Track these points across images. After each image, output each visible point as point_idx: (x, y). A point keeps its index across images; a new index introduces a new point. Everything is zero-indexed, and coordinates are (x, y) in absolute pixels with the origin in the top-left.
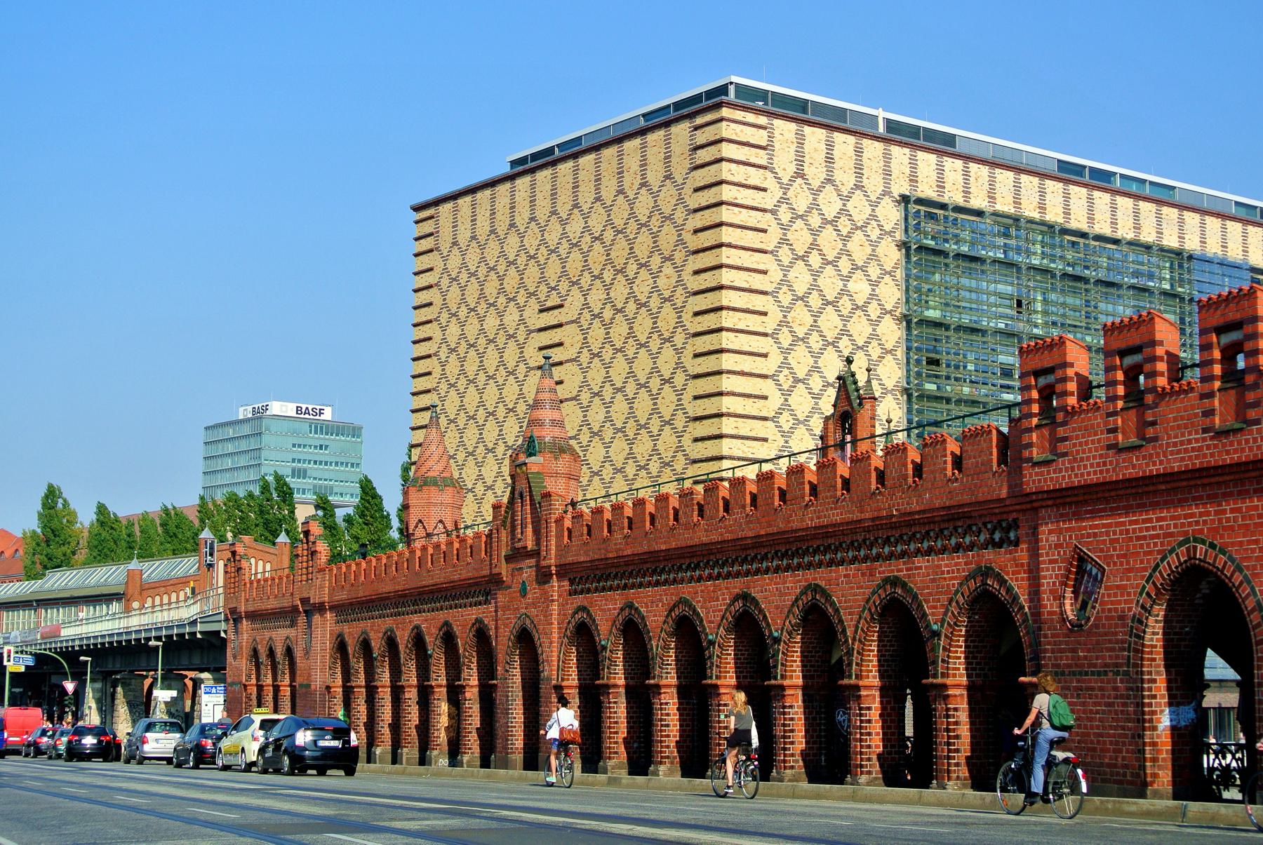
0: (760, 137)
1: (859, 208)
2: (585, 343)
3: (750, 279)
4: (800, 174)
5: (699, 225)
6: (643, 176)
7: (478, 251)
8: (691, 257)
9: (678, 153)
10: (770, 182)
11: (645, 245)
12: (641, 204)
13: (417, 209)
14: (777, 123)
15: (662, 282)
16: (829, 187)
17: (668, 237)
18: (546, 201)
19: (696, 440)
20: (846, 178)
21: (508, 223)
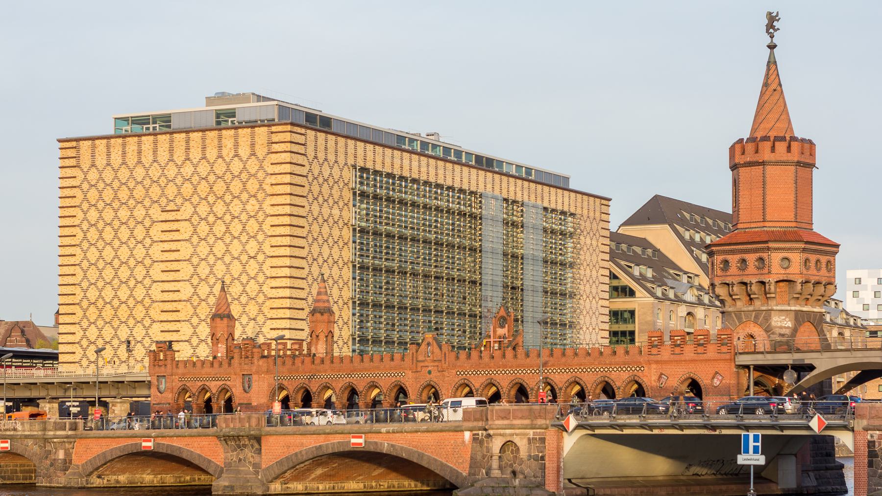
0: (301, 139)
1: (336, 172)
2: (195, 231)
3: (298, 210)
4: (316, 157)
5: (274, 182)
6: (236, 151)
7: (112, 172)
8: (269, 198)
9: (260, 142)
10: (305, 163)
11: (238, 187)
12: (235, 166)
13: (60, 141)
14: (309, 131)
15: (249, 207)
16: (326, 163)
17: (253, 185)
18: (166, 153)
19: (272, 288)
20: (331, 157)
21: (136, 160)
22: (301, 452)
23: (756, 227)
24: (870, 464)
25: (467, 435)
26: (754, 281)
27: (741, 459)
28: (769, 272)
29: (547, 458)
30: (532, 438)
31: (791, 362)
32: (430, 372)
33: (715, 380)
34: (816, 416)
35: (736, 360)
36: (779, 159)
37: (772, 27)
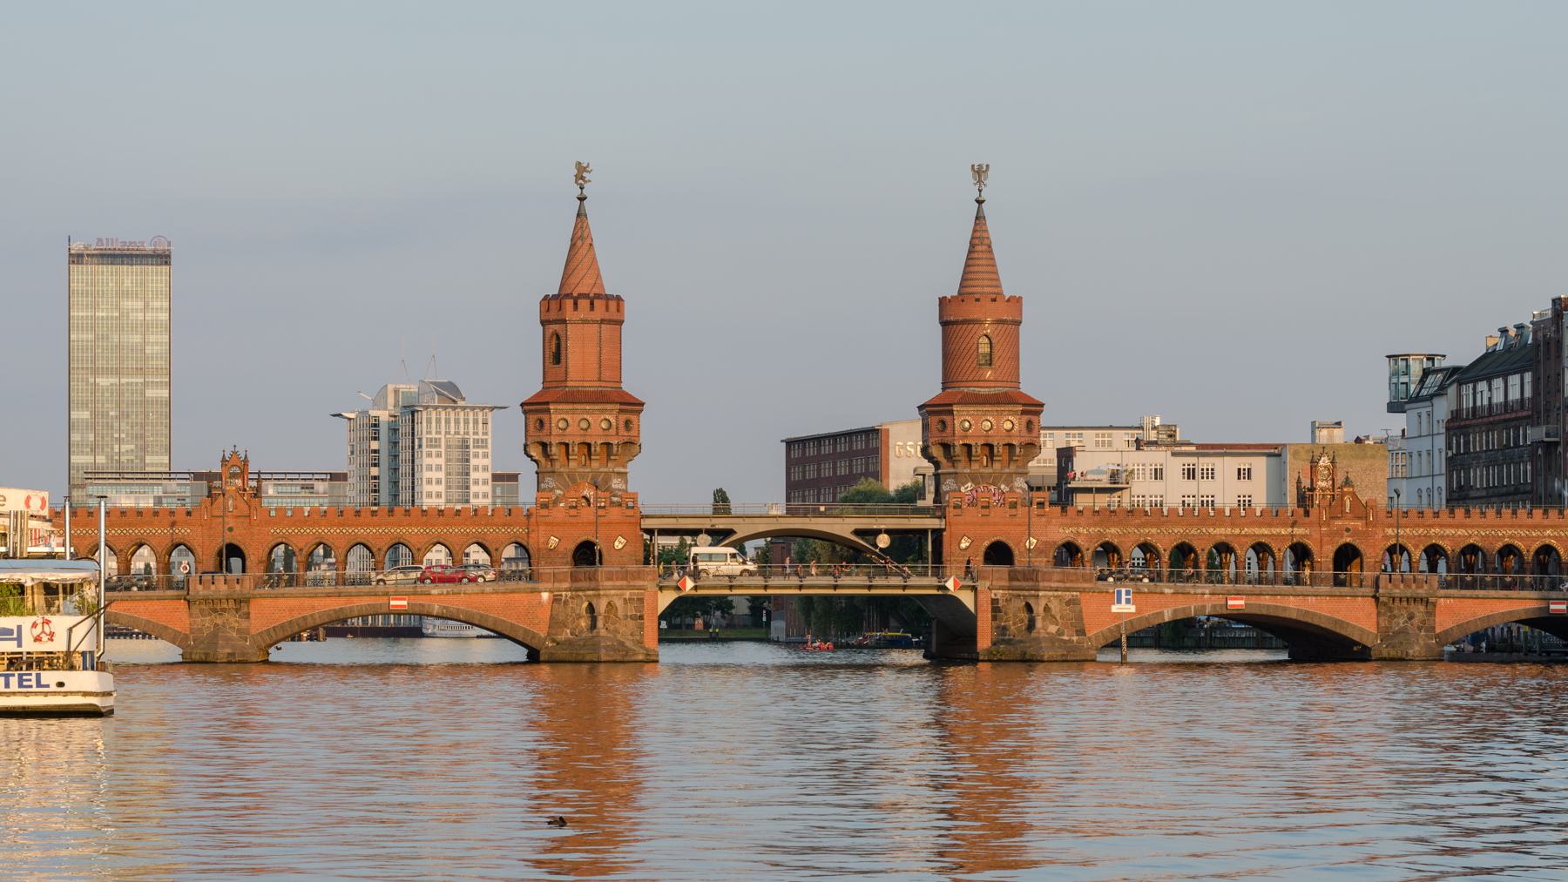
22: (312, 616)
23: (592, 386)
24: (994, 618)
25: (545, 596)
26: (599, 442)
27: (1115, 609)
28: (617, 434)
29: (645, 617)
30: (629, 599)
31: (709, 527)
32: (231, 529)
33: (616, 543)
34: (952, 579)
35: (642, 523)
36: (611, 318)
37: (582, 178)
